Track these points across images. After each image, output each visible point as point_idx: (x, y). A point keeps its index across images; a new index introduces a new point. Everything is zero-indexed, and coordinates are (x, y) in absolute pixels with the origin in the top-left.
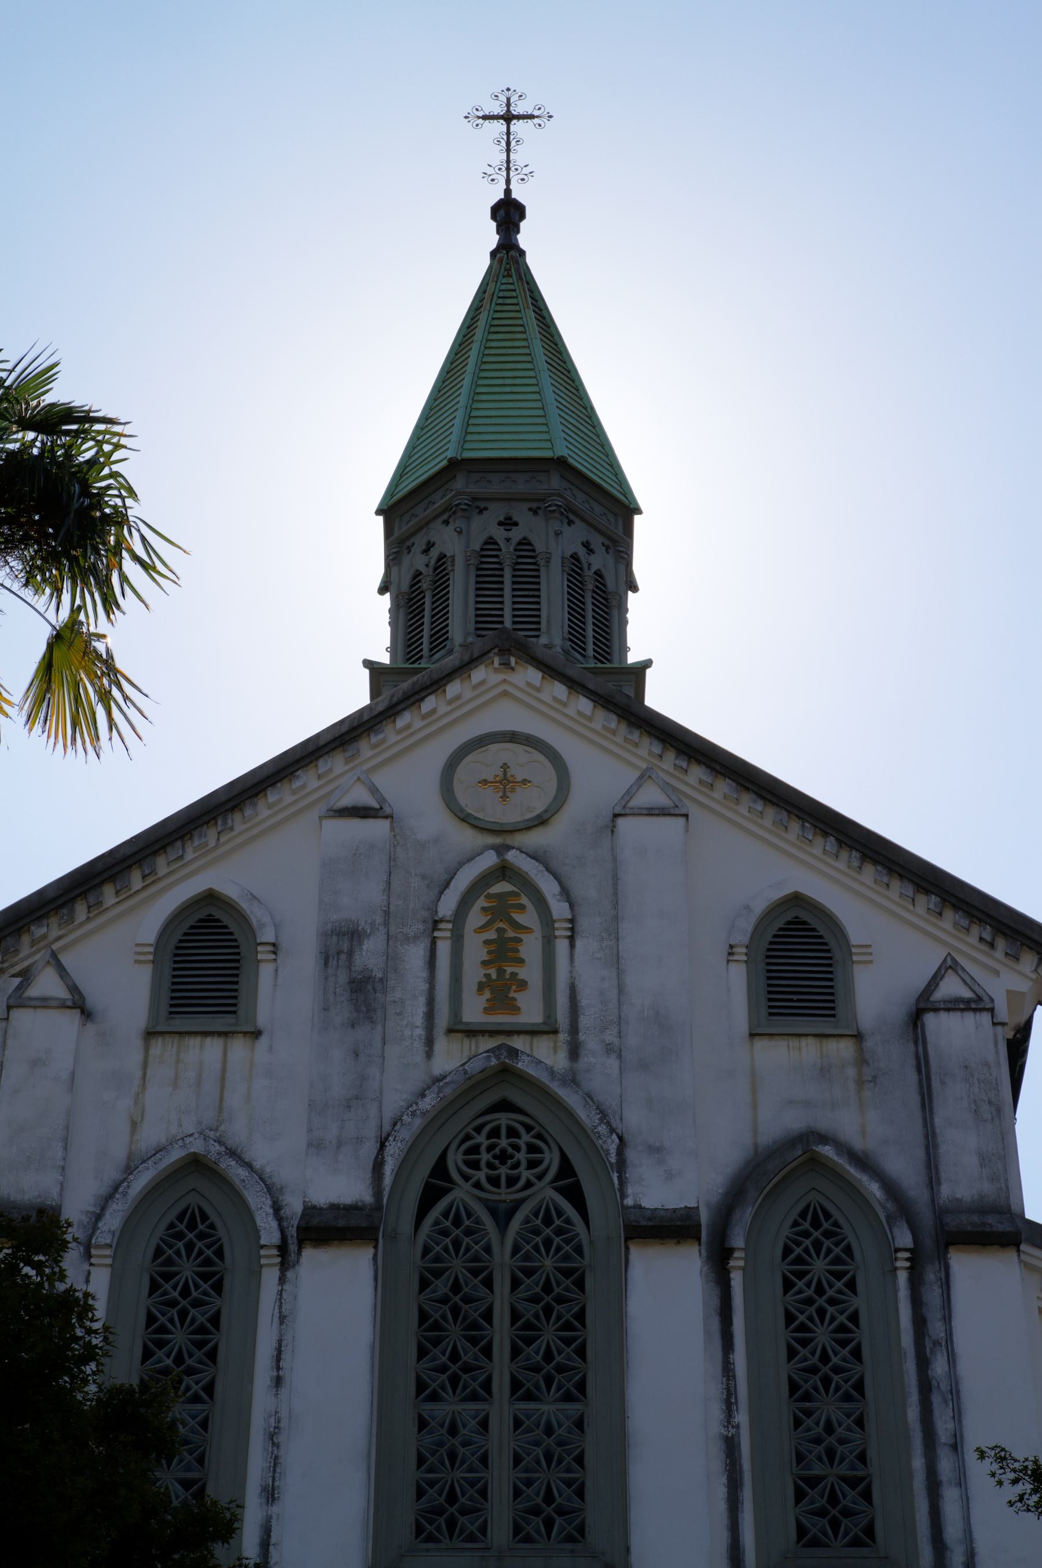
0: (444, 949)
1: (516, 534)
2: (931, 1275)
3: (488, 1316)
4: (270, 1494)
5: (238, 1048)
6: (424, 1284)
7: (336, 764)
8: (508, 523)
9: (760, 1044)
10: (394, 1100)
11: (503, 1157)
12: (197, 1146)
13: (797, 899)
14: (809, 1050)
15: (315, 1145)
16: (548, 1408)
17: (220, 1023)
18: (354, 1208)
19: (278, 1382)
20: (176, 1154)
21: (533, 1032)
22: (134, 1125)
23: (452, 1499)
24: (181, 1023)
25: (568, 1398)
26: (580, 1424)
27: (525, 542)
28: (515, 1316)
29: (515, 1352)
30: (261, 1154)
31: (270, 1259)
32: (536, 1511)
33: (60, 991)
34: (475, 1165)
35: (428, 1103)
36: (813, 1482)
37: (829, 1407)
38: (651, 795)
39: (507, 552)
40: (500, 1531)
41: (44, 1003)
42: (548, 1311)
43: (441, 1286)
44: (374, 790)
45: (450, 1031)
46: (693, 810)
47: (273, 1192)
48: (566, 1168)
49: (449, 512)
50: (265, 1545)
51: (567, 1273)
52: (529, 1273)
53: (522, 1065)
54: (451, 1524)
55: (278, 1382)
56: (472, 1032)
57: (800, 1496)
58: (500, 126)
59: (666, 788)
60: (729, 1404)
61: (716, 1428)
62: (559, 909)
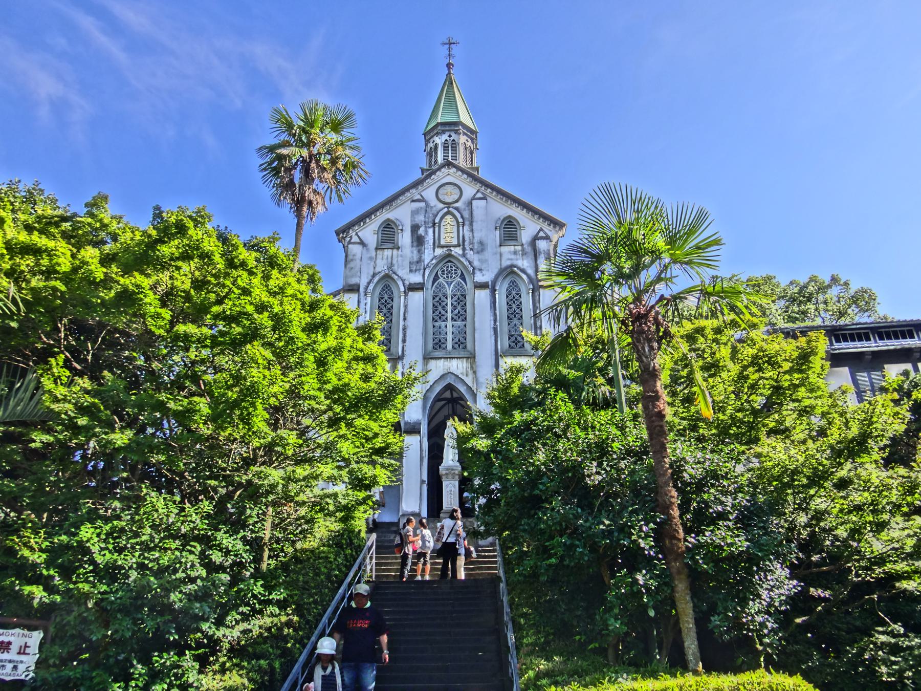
0: (437, 229)
1: (452, 138)
2: (537, 294)
3: (447, 305)
4: (404, 341)
5: (395, 251)
6: (434, 299)
7: (413, 191)
8: (450, 136)
9: (502, 247)
11: (449, 272)
12: (387, 272)
13: (510, 217)
14: (512, 248)
15: (411, 271)
16: (459, 323)
17: (391, 246)
18: (419, 284)
20: (383, 274)
21: (455, 246)
22: (374, 268)
23: (440, 341)
24: (384, 246)
25: (463, 321)
26: (465, 326)
27: (454, 140)
28: (452, 304)
29: (452, 312)
30: (400, 273)
31: (402, 294)
32: (456, 343)
33: (358, 240)
34: (444, 274)
35: (434, 261)
36: (512, 336)
37: (515, 321)
38: (479, 195)
39: (450, 142)
40: (450, 347)
41: (354, 243)
42: (459, 303)
43: (437, 299)
44: (421, 196)
45: (438, 247)
46: (488, 198)
47: (403, 281)
48: (462, 274)
49: (437, 134)
51: (462, 295)
52: (455, 295)
53: (453, 253)
54: (440, 346)
55: (405, 319)
56: (442, 247)
57: (509, 339)
58: (448, 46)
59: (482, 193)
60: (495, 321)
61: (492, 326)
62: (460, 220)
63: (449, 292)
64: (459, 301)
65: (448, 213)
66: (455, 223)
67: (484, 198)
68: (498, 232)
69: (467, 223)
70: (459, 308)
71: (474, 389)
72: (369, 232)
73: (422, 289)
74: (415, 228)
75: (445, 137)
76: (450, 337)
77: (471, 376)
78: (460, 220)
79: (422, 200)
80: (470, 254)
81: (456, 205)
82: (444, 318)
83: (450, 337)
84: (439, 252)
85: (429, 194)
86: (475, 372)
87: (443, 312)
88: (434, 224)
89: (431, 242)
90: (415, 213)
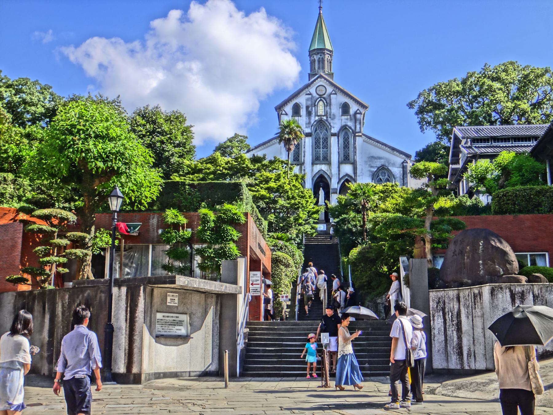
1: (322, 57)
4: (304, 157)
5: (300, 117)
7: (307, 90)
10: (312, 122)
14: (346, 117)
15: (306, 127)
16: (325, 150)
17: (298, 115)
19: (304, 148)
21: (324, 116)
33: (285, 113)
35: (315, 123)
38: (334, 92)
39: (321, 59)
41: (284, 114)
46: (338, 94)
48: (326, 128)
49: (315, 54)
50: (304, 161)
55: (304, 148)
56: (318, 116)
59: (335, 91)
60: (339, 149)
63: (321, 137)
64: (325, 140)
65: (321, 100)
66: (323, 105)
67: (336, 94)
68: (341, 109)
69: (328, 105)
70: (325, 143)
71: (330, 176)
72: (289, 109)
73: (311, 136)
74: (307, 107)
75: (319, 56)
76: (321, 156)
77: (329, 171)
78: (326, 104)
79: (310, 94)
80: (329, 119)
81: (324, 96)
82: (319, 147)
83: (321, 156)
84: (317, 118)
85: (312, 90)
86: (331, 170)
87: (319, 145)
88: (315, 105)
89: (314, 114)
90: (307, 100)
